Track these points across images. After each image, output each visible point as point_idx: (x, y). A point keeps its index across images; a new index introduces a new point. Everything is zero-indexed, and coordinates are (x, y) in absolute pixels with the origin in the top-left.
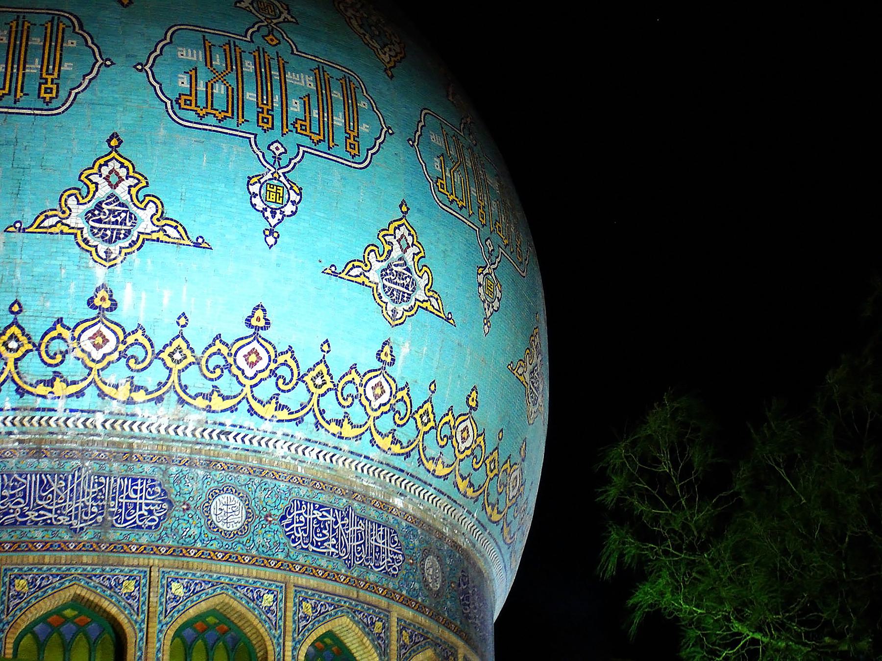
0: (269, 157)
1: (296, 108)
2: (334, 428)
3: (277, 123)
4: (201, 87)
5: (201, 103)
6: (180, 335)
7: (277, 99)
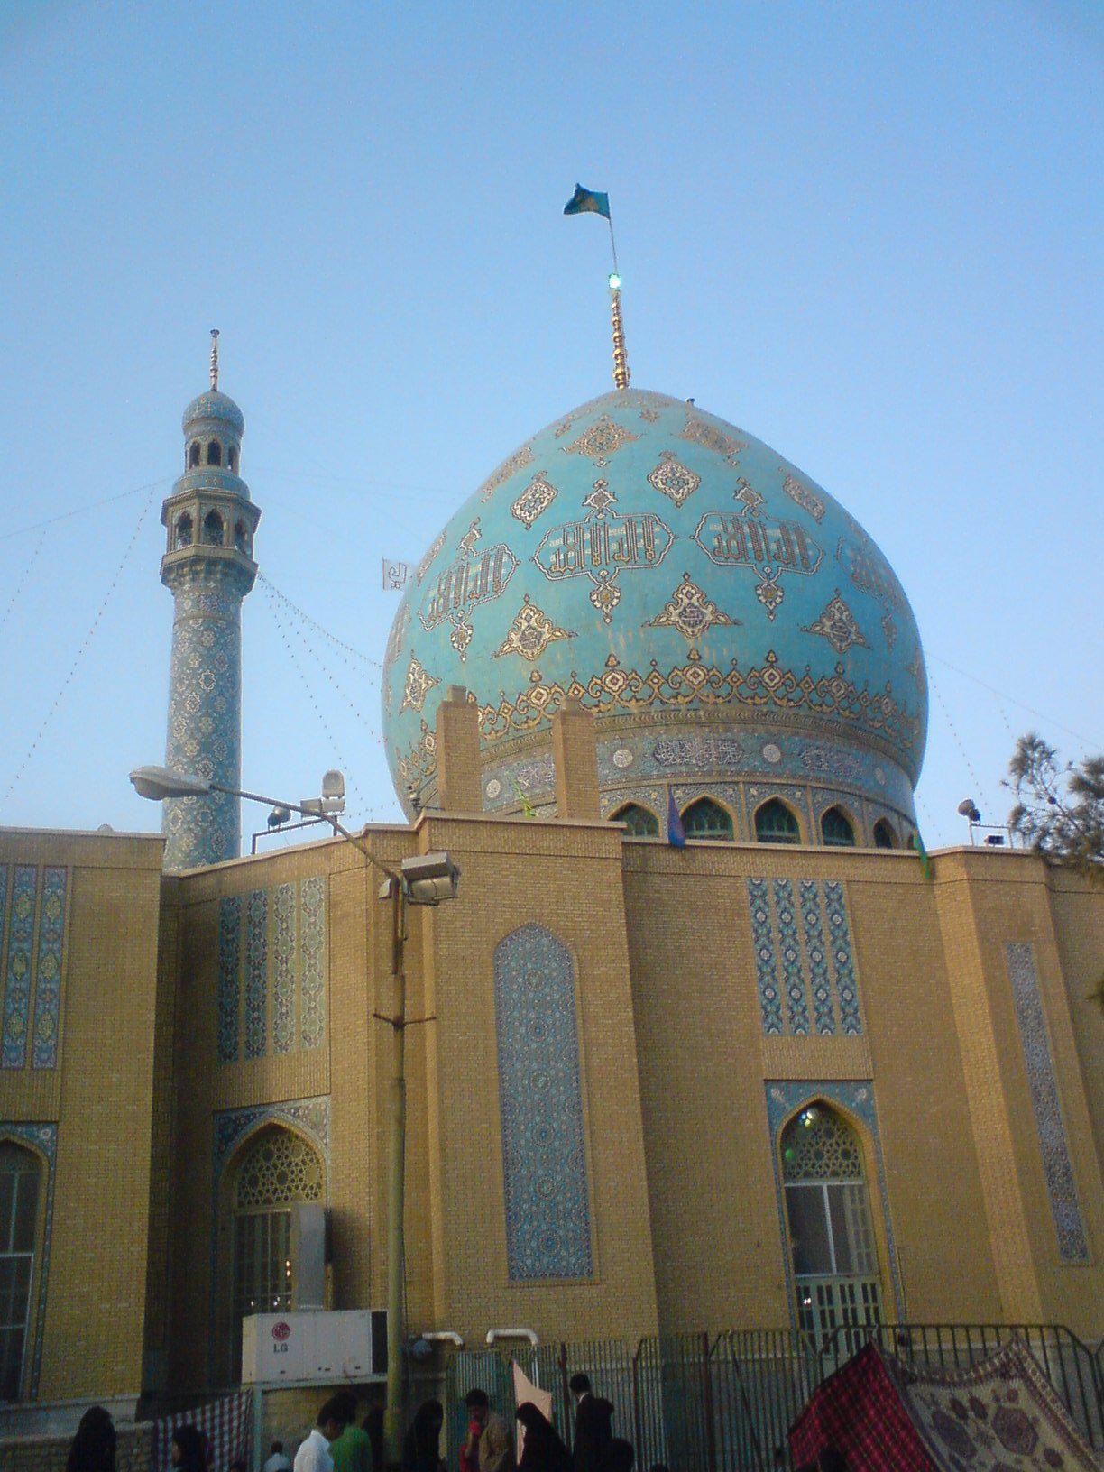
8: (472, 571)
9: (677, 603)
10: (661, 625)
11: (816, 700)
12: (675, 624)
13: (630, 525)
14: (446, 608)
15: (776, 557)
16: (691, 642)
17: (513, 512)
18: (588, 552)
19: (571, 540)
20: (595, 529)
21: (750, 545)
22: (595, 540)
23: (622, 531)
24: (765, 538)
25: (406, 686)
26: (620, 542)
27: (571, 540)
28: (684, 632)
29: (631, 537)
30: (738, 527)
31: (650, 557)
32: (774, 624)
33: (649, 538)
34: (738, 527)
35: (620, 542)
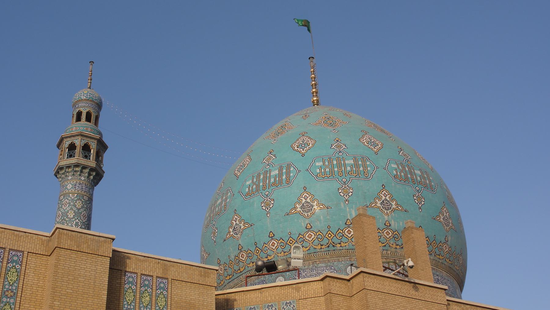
0: (342, 182)
1: (349, 168)
2: (438, 256)
3: (344, 174)
4: (323, 171)
5: (323, 174)
6: (290, 237)
7: (343, 168)
8: (273, 173)
9: (380, 199)
10: (372, 207)
11: (438, 253)
12: (379, 208)
13: (355, 160)
14: (257, 190)
15: (420, 183)
16: (386, 217)
17: (294, 149)
18: (336, 169)
19: (327, 163)
20: (338, 159)
21: (409, 176)
22: (339, 165)
23: (352, 162)
24: (415, 174)
25: (231, 227)
26: (351, 167)
27: (327, 163)
28: (383, 212)
29: (357, 165)
30: (404, 168)
31: (367, 176)
32: (422, 213)
33: (365, 167)
34: (404, 168)
35: (351, 167)
